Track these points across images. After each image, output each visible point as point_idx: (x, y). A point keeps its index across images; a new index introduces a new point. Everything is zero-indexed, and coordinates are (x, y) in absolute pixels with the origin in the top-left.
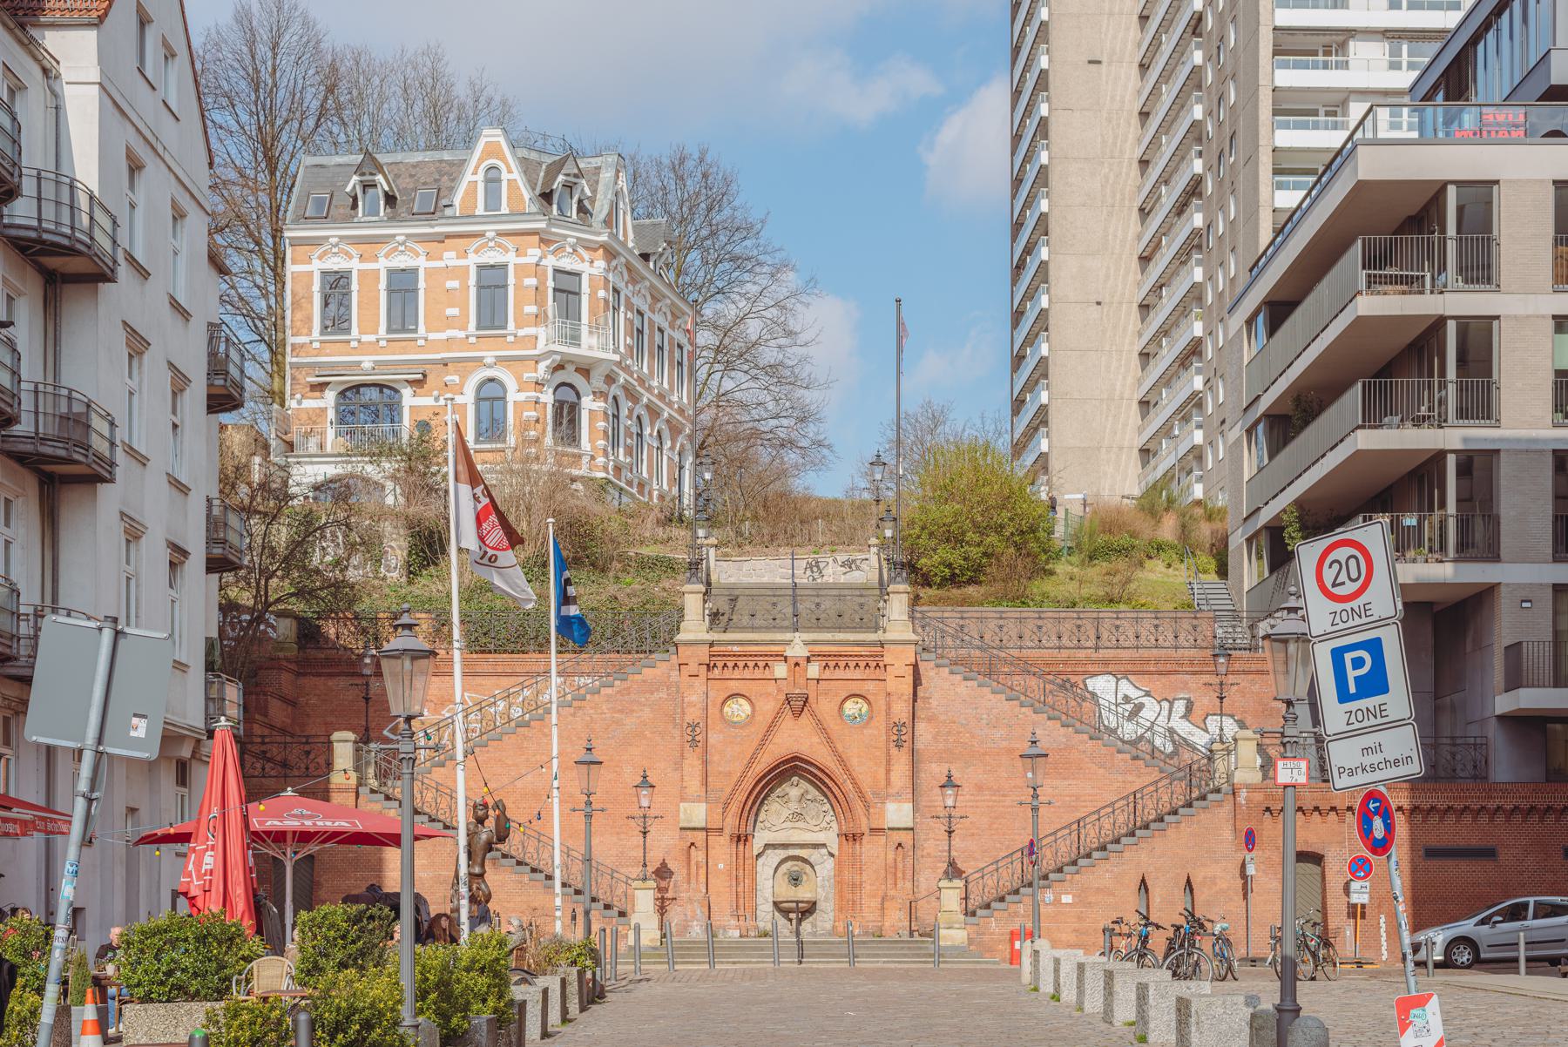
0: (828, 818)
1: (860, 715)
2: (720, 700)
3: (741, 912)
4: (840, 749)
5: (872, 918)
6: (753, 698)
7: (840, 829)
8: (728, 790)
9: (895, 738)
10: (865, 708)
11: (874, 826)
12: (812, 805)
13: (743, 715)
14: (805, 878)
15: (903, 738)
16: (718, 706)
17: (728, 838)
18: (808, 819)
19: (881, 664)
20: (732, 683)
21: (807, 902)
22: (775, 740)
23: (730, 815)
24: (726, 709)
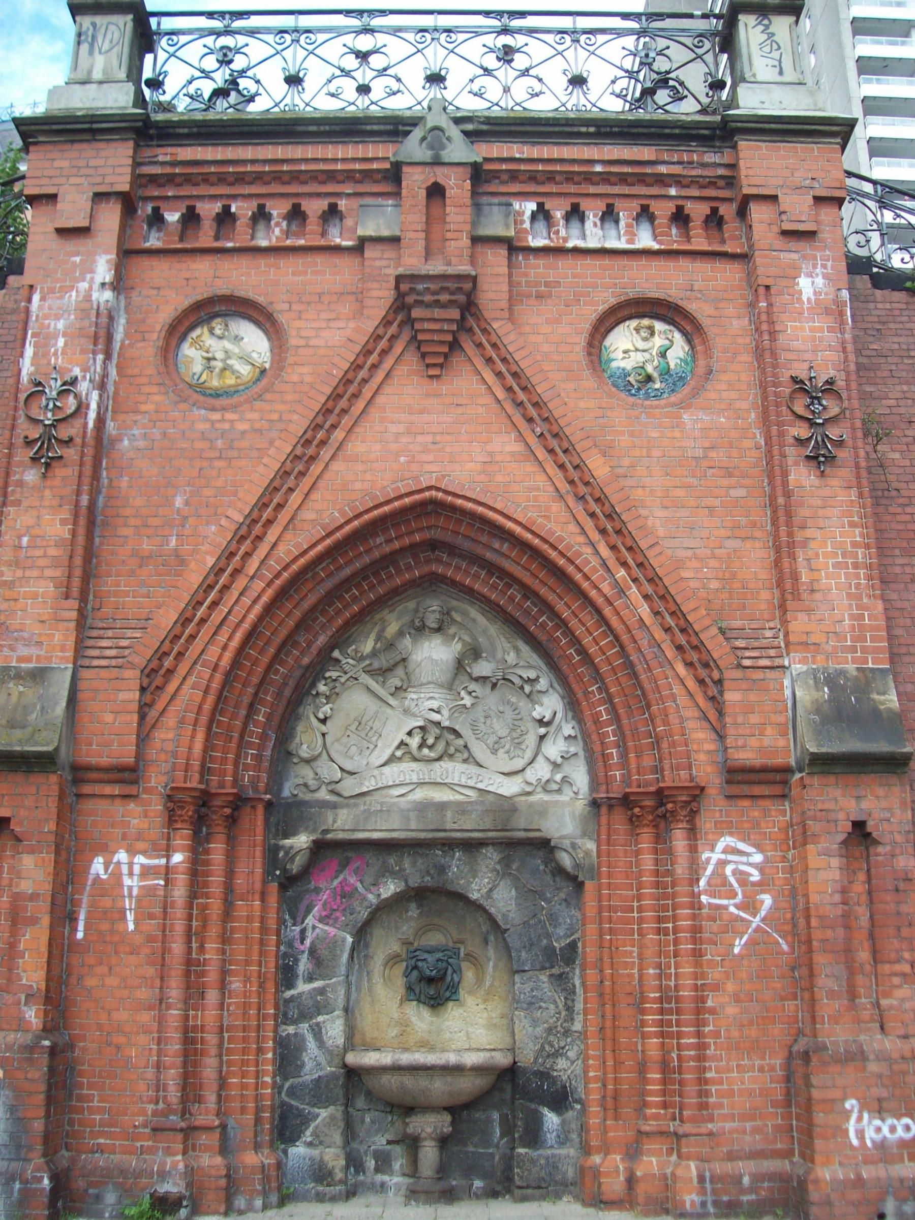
0: (554, 749)
1: (666, 373)
2: (165, 315)
3: (206, 1115)
4: (598, 466)
5: (751, 1141)
6: (279, 308)
7: (594, 783)
8: (168, 618)
9: (802, 431)
10: (679, 350)
11: (746, 756)
12: (492, 700)
13: (245, 370)
14: (469, 975)
15: (833, 433)
16: (156, 336)
17: (157, 806)
18: (479, 750)
19: (726, 210)
20: (202, 267)
21: (478, 1070)
22: (356, 447)
23: (170, 720)
24: (188, 350)
